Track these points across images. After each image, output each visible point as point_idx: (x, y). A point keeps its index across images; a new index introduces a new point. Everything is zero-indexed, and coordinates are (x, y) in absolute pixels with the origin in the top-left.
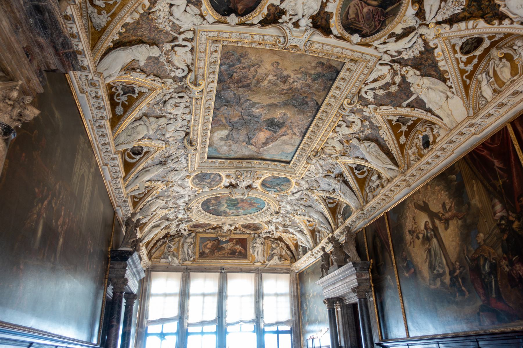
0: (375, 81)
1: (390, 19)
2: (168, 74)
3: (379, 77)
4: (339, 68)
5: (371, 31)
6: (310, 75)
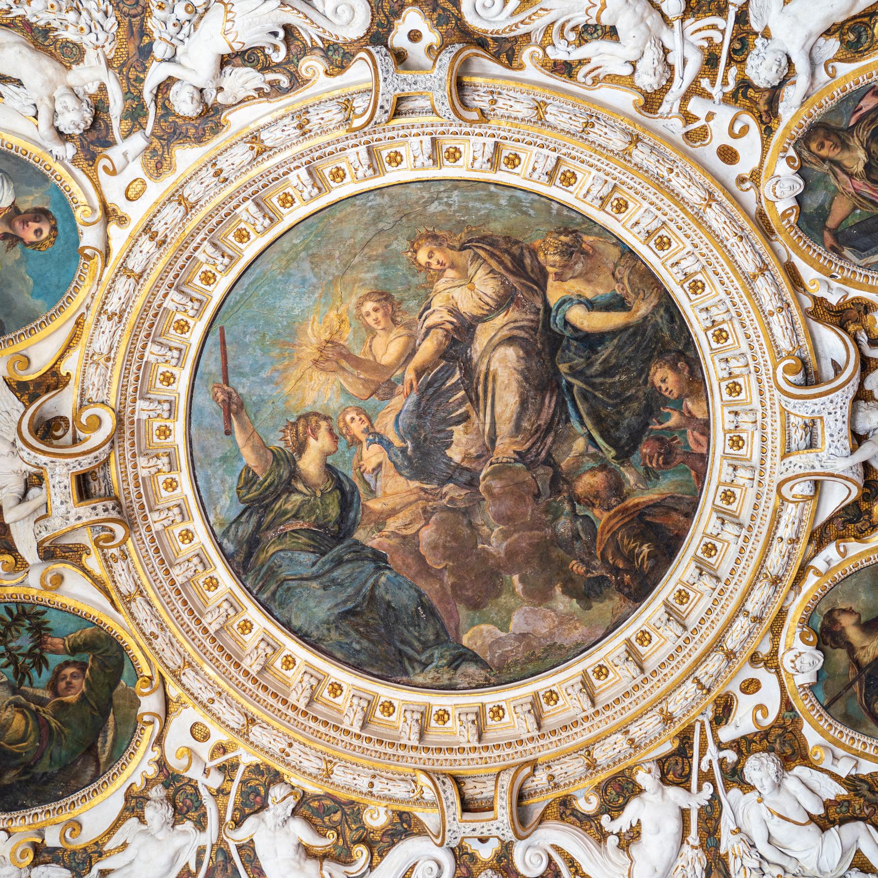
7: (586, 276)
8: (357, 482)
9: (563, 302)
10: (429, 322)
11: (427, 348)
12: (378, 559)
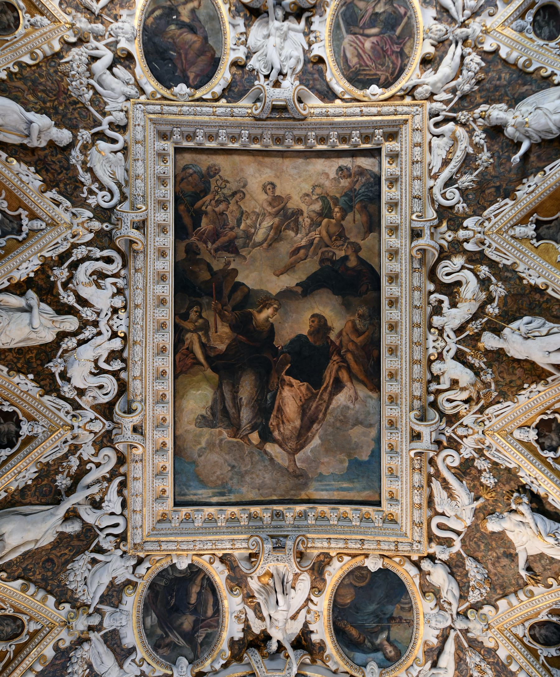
0: (446, 163)
1: (408, 44)
2: (86, 199)
3: (449, 152)
4: (376, 170)
5: (392, 74)
6: (336, 201)
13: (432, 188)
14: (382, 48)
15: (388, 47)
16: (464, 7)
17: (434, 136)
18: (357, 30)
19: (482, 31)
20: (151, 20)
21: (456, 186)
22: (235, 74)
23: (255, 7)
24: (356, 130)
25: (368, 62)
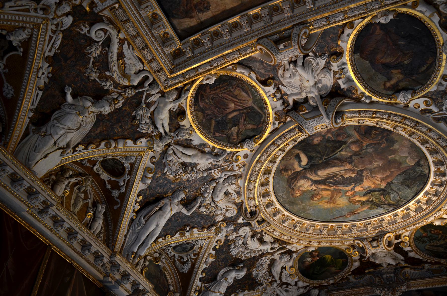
0: (121, 55)
1: (201, 118)
3: (124, 63)
4: (175, 22)
7: (292, 165)
8: (367, 190)
9: (301, 166)
10: (316, 189)
11: (323, 187)
12: (389, 184)
13: (119, 32)
14: (219, 108)
15: (216, 110)
16: (175, 154)
17: (144, 70)
18: (245, 111)
19: (153, 148)
20: (429, 62)
21: (100, 43)
22: (336, 47)
23: (334, 100)
24: (209, 48)
25: (226, 95)
